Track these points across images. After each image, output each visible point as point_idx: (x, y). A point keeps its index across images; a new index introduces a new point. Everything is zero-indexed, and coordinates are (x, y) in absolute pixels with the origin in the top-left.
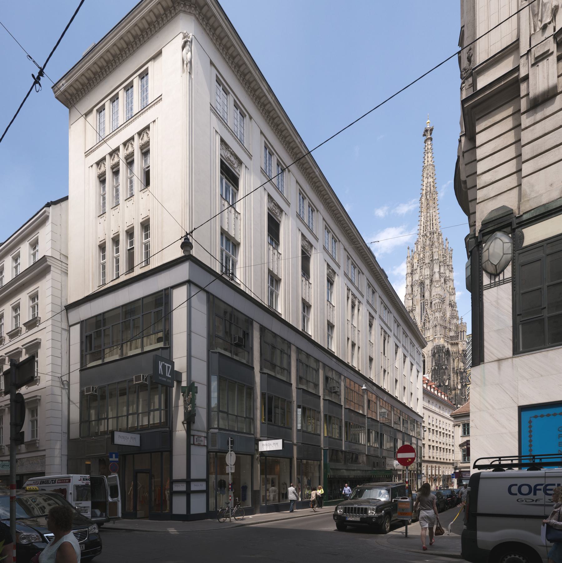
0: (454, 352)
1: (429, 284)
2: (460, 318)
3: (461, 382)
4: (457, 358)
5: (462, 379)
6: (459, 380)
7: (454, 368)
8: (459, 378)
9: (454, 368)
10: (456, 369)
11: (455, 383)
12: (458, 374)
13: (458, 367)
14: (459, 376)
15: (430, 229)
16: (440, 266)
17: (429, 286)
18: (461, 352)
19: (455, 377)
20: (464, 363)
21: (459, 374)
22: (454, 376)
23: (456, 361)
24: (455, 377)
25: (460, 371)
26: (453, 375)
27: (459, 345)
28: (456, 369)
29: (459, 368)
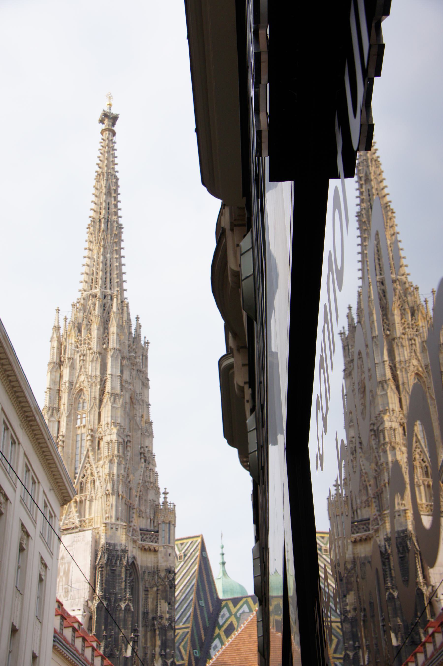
0: (147, 572)
1: (98, 397)
2: (162, 491)
3: (161, 655)
4: (155, 589)
5: (164, 646)
6: (158, 649)
7: (146, 614)
8: (158, 643)
9: (146, 614)
10: (150, 616)
11: (149, 656)
12: (155, 630)
13: (156, 612)
14: (157, 638)
15: (106, 287)
16: (122, 366)
17: (98, 401)
18: (163, 574)
19: (149, 640)
20: (169, 604)
21: (157, 632)
22: (145, 636)
23: (151, 596)
24: (149, 640)
25: (160, 623)
26: (143, 633)
27: (160, 555)
28: (150, 616)
29: (159, 614)
